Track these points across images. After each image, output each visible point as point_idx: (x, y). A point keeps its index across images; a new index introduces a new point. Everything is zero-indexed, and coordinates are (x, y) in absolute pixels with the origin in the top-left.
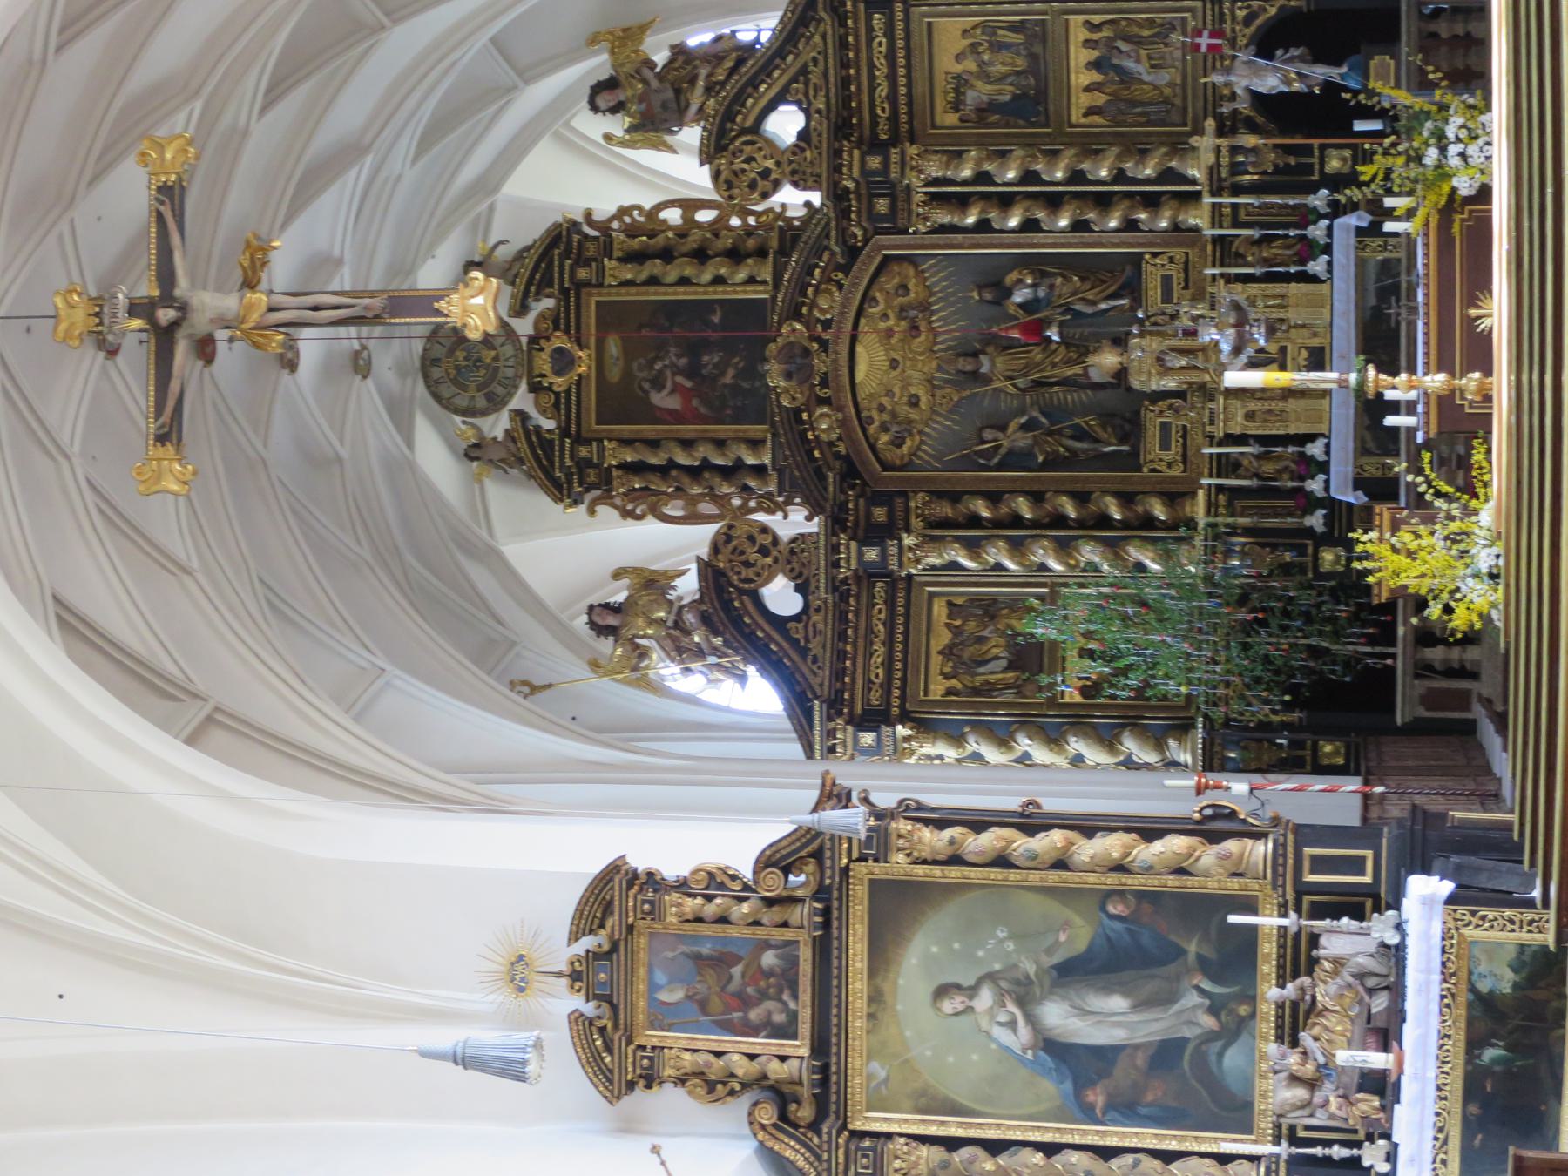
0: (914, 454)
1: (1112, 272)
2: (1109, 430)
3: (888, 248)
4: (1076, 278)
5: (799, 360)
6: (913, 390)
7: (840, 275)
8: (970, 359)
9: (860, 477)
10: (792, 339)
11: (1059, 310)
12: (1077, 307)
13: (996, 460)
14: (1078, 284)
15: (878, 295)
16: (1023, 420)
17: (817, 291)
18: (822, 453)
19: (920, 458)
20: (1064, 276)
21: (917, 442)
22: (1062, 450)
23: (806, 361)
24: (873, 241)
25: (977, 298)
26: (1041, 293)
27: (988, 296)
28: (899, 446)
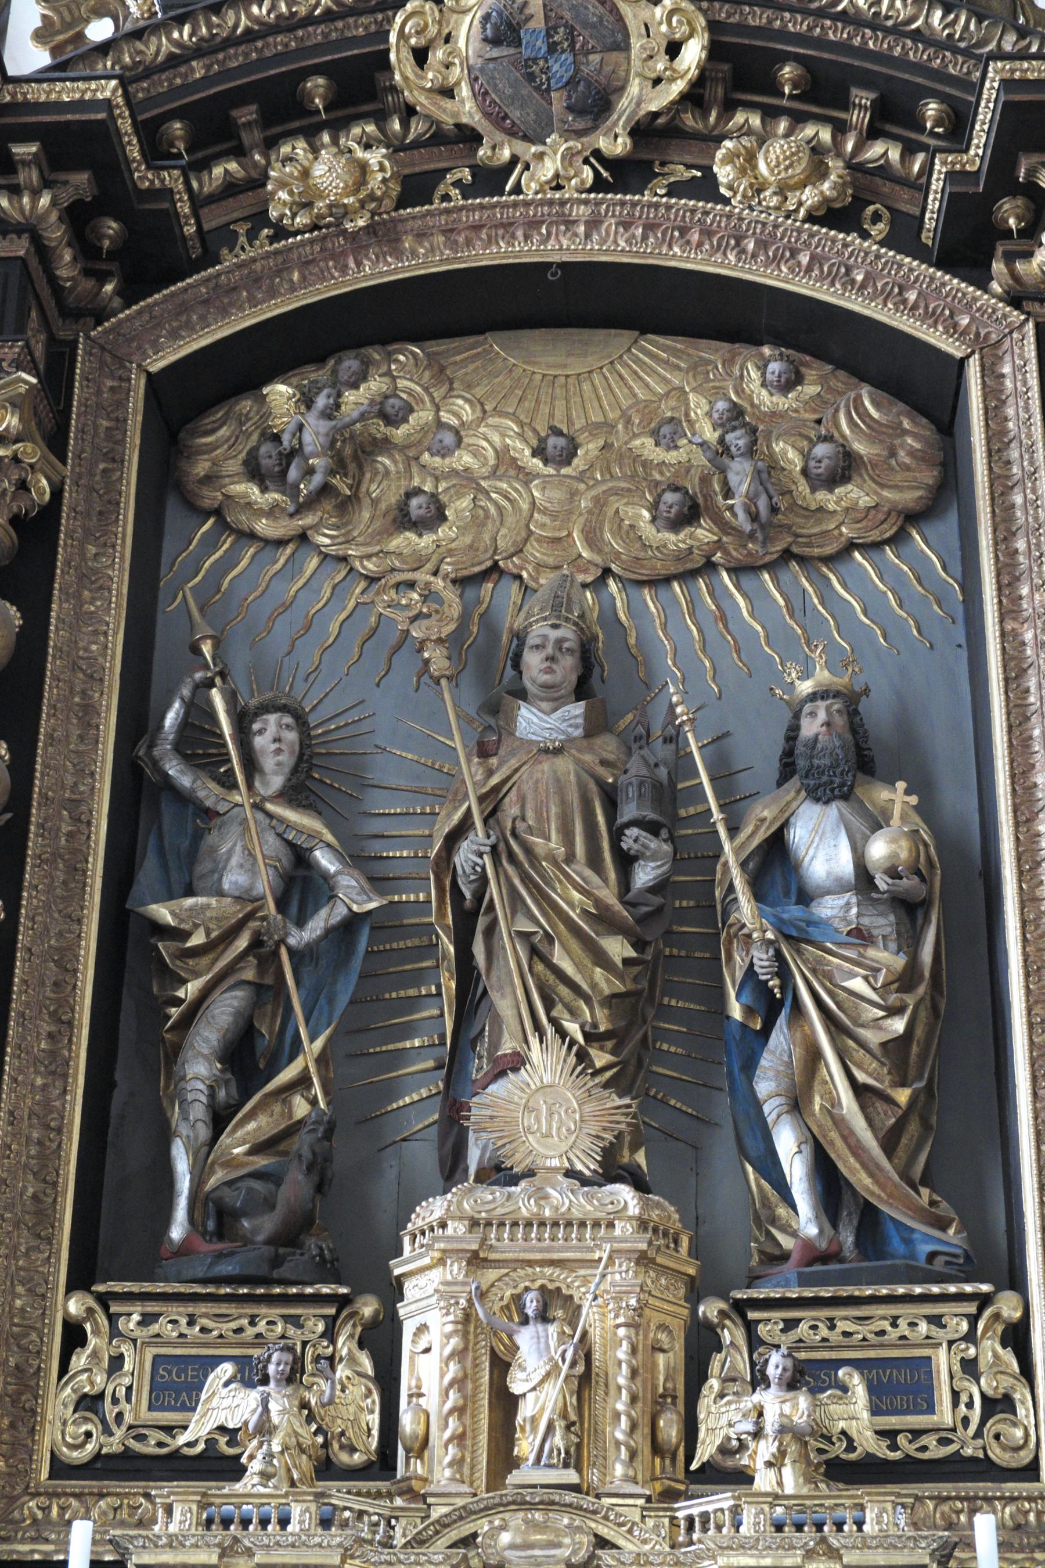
0: (224, 526)
1: (925, 1180)
2: (261, 1162)
3: (990, 372)
4: (898, 1025)
5: (560, 67)
6: (458, 508)
7: (880, 230)
8: (567, 667)
9: (129, 295)
10: (637, 44)
11: (762, 959)
12: (780, 1038)
13: (174, 769)
14: (872, 1038)
15: (810, 390)
16: (325, 860)
17: (817, 150)
18: (231, 188)
19: (210, 543)
20: (907, 980)
21: (263, 526)
22: (190, 990)
23: (558, 101)
24: (1016, 316)
25: (806, 687)
26: (829, 908)
27: (810, 727)
28: (254, 472)
